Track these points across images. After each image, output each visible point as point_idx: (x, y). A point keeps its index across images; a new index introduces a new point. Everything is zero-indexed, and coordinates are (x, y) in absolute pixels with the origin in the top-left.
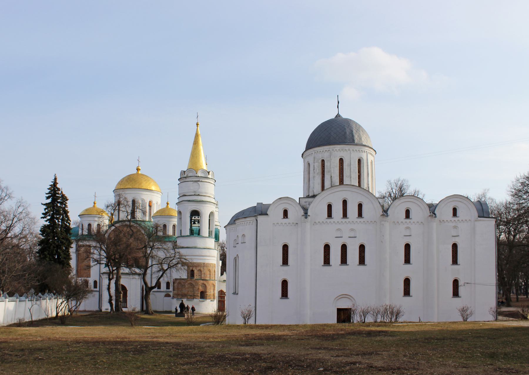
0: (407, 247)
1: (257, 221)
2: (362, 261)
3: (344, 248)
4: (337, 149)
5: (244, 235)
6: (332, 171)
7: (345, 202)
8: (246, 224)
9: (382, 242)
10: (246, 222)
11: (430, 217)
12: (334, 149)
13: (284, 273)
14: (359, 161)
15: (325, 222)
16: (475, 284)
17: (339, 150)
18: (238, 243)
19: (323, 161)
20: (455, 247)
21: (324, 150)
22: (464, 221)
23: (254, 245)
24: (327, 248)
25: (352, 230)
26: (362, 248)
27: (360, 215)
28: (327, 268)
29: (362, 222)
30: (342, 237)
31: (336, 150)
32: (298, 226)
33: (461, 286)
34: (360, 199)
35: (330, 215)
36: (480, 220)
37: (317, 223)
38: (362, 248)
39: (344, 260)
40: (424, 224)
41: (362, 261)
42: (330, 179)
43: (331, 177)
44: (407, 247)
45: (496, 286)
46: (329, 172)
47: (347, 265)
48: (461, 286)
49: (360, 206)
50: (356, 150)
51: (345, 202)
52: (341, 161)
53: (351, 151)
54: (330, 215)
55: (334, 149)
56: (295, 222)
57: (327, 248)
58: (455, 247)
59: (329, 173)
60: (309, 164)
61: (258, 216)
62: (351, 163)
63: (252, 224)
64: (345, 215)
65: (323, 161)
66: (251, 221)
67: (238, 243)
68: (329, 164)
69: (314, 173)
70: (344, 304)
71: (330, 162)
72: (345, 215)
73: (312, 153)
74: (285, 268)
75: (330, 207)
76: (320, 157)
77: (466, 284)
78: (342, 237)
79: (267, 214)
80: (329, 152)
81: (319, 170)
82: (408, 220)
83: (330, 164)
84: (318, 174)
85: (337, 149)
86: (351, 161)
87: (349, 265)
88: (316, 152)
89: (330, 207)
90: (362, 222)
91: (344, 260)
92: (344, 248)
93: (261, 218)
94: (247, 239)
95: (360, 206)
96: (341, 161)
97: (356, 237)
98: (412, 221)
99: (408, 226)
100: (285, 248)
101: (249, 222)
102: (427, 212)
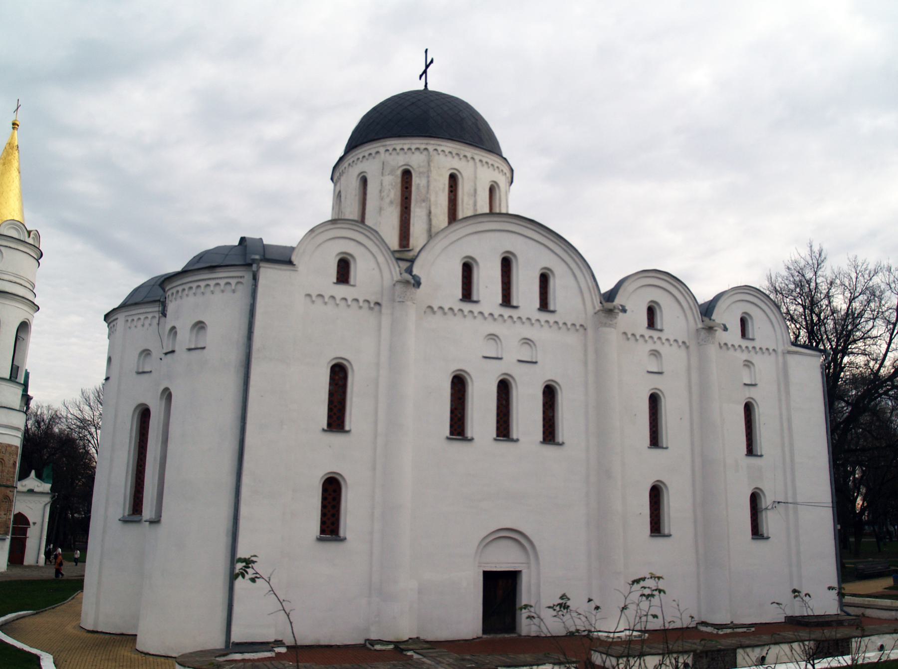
0: (654, 400)
1: (255, 278)
2: (550, 434)
3: (504, 388)
4: (447, 150)
5: (200, 326)
6: (433, 199)
7: (507, 264)
10: (212, 283)
12: (440, 149)
15: (456, 310)
16: (795, 503)
17: (450, 152)
18: (173, 352)
19: (407, 175)
20: (749, 408)
21: (413, 147)
22: (771, 351)
23: (234, 355)
24: (459, 384)
25: (527, 341)
26: (550, 393)
27: (544, 305)
28: (458, 447)
29: (552, 321)
30: (501, 359)
31: (443, 151)
32: (380, 311)
33: (766, 509)
34: (547, 260)
35: (467, 295)
37: (436, 309)
38: (550, 393)
39: (504, 430)
40: (687, 347)
41: (550, 434)
42: (424, 217)
43: (430, 212)
44: (654, 400)
45: (833, 507)
46: (426, 200)
47: (513, 440)
48: (766, 509)
49: (544, 279)
50: (487, 163)
51: (507, 264)
52: (453, 179)
53: (477, 161)
54: (467, 295)
55: (440, 149)
56: (373, 299)
57: (459, 384)
58: (749, 408)
59: (424, 204)
61: (262, 264)
62: (475, 191)
63: (234, 291)
64: (507, 300)
65: (407, 175)
66: (233, 282)
67: (173, 352)
68: (423, 182)
69: (382, 199)
71: (428, 177)
72: (507, 300)
73: (378, 152)
74: (336, 439)
75: (468, 269)
76: (400, 161)
77: (776, 504)
78: (501, 359)
80: (425, 153)
81: (394, 193)
83: (428, 182)
84: (391, 202)
85: (447, 150)
86: (475, 184)
87: (517, 440)
88: (390, 148)
89: (468, 269)
90: (552, 321)
91: (504, 430)
92: (504, 388)
93: (268, 274)
94: (211, 337)
95: (544, 279)
96: (453, 179)
97: (536, 363)
101: (222, 282)
102: (695, 321)
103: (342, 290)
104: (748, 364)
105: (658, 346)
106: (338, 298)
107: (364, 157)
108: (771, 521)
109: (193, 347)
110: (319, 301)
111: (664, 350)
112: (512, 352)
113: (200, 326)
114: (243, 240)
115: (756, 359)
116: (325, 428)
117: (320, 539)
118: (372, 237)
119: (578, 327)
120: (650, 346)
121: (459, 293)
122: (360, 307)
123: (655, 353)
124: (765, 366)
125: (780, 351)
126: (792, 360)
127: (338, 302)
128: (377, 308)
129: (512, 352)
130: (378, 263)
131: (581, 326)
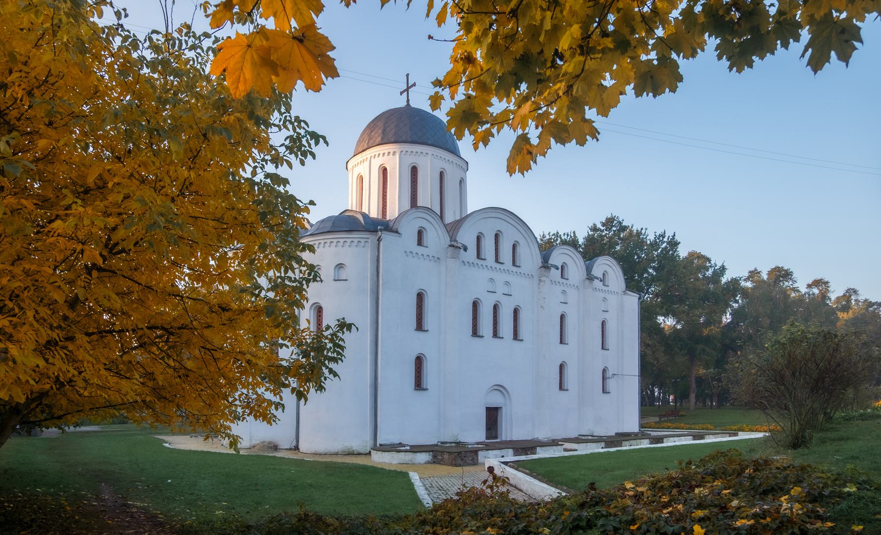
0: (562, 317)
1: (379, 240)
3: (496, 308)
8: (322, 245)
9: (542, 307)
10: (349, 241)
11: (587, 281)
13: (418, 343)
15: (475, 263)
24: (475, 305)
25: (507, 283)
26: (516, 312)
32: (439, 262)
36: (627, 294)
38: (516, 312)
40: (579, 289)
41: (516, 336)
57: (475, 305)
66: (363, 241)
70: (495, 400)
79: (397, 232)
92: (496, 308)
95: (514, 247)
97: (511, 295)
100: (420, 297)
103: (420, 250)
104: (605, 299)
106: (420, 254)
107: (384, 154)
108: (611, 384)
110: (410, 255)
111: (568, 290)
112: (501, 289)
113: (340, 266)
115: (609, 296)
117: (415, 389)
118: (435, 218)
119: (489, 268)
122: (430, 260)
123: (564, 292)
124: (613, 300)
126: (626, 298)
128: (438, 261)
129: (501, 289)
130: (438, 234)
131: (532, 275)
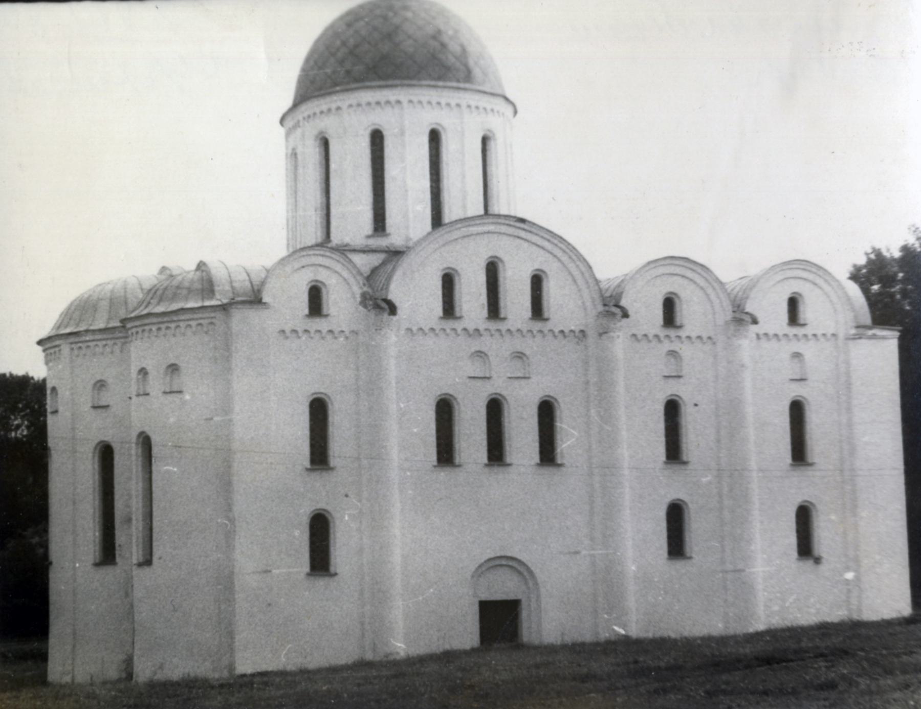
7: (492, 271)
14: (485, 141)
27: (538, 309)
35: (449, 309)
49: (537, 282)
51: (492, 271)
54: (449, 309)
60: (325, 144)
64: (494, 309)
72: (494, 309)
75: (448, 282)
82: (672, 333)
89: (448, 282)
95: (537, 282)
96: (435, 137)
98: (683, 333)
99: (673, 347)
105: (676, 346)
106: (312, 331)
109: (168, 390)
111: (686, 350)
114: (201, 266)
116: (309, 466)
120: (667, 346)
121: (439, 311)
123: (673, 353)
125: (841, 335)
127: (312, 335)
